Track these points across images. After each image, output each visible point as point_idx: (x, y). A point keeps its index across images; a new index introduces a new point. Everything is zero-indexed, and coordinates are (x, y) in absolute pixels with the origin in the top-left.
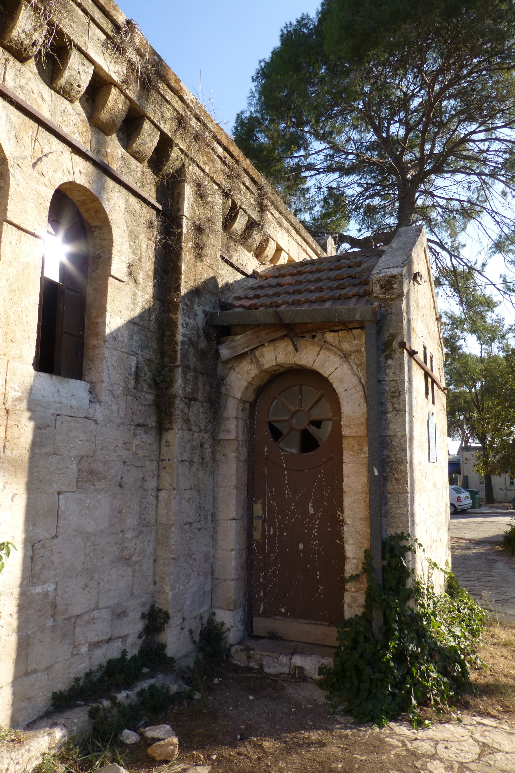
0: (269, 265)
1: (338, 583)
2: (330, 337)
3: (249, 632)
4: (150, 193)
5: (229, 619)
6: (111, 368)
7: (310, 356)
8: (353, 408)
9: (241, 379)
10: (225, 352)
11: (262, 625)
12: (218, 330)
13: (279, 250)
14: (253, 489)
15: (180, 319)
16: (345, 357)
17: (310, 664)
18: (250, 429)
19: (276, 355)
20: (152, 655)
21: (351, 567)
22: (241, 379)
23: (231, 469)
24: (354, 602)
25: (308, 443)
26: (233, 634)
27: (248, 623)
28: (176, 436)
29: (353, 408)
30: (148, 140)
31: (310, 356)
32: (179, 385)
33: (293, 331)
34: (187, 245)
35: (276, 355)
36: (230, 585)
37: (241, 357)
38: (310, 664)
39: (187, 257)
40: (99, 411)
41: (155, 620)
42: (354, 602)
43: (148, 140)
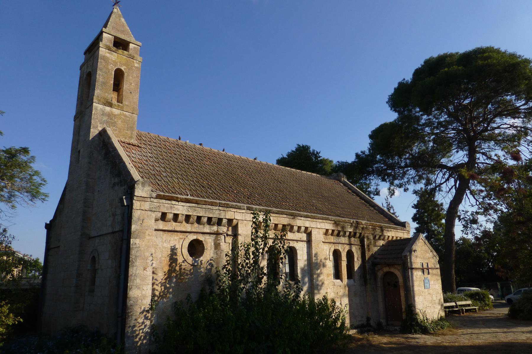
0: (386, 241)
2: (396, 266)
4: (359, 243)
5: (382, 321)
6: (356, 277)
7: (392, 270)
8: (401, 280)
9: (380, 274)
10: (376, 269)
12: (374, 265)
13: (389, 237)
15: (367, 265)
16: (399, 270)
17: (397, 328)
19: (386, 269)
20: (369, 325)
21: (403, 310)
22: (380, 274)
24: (404, 316)
29: (401, 280)
30: (358, 235)
33: (389, 265)
34: (366, 250)
35: (386, 269)
37: (379, 270)
38: (397, 328)
39: (367, 252)
40: (356, 284)
41: (368, 319)
42: (404, 316)
43: (358, 235)
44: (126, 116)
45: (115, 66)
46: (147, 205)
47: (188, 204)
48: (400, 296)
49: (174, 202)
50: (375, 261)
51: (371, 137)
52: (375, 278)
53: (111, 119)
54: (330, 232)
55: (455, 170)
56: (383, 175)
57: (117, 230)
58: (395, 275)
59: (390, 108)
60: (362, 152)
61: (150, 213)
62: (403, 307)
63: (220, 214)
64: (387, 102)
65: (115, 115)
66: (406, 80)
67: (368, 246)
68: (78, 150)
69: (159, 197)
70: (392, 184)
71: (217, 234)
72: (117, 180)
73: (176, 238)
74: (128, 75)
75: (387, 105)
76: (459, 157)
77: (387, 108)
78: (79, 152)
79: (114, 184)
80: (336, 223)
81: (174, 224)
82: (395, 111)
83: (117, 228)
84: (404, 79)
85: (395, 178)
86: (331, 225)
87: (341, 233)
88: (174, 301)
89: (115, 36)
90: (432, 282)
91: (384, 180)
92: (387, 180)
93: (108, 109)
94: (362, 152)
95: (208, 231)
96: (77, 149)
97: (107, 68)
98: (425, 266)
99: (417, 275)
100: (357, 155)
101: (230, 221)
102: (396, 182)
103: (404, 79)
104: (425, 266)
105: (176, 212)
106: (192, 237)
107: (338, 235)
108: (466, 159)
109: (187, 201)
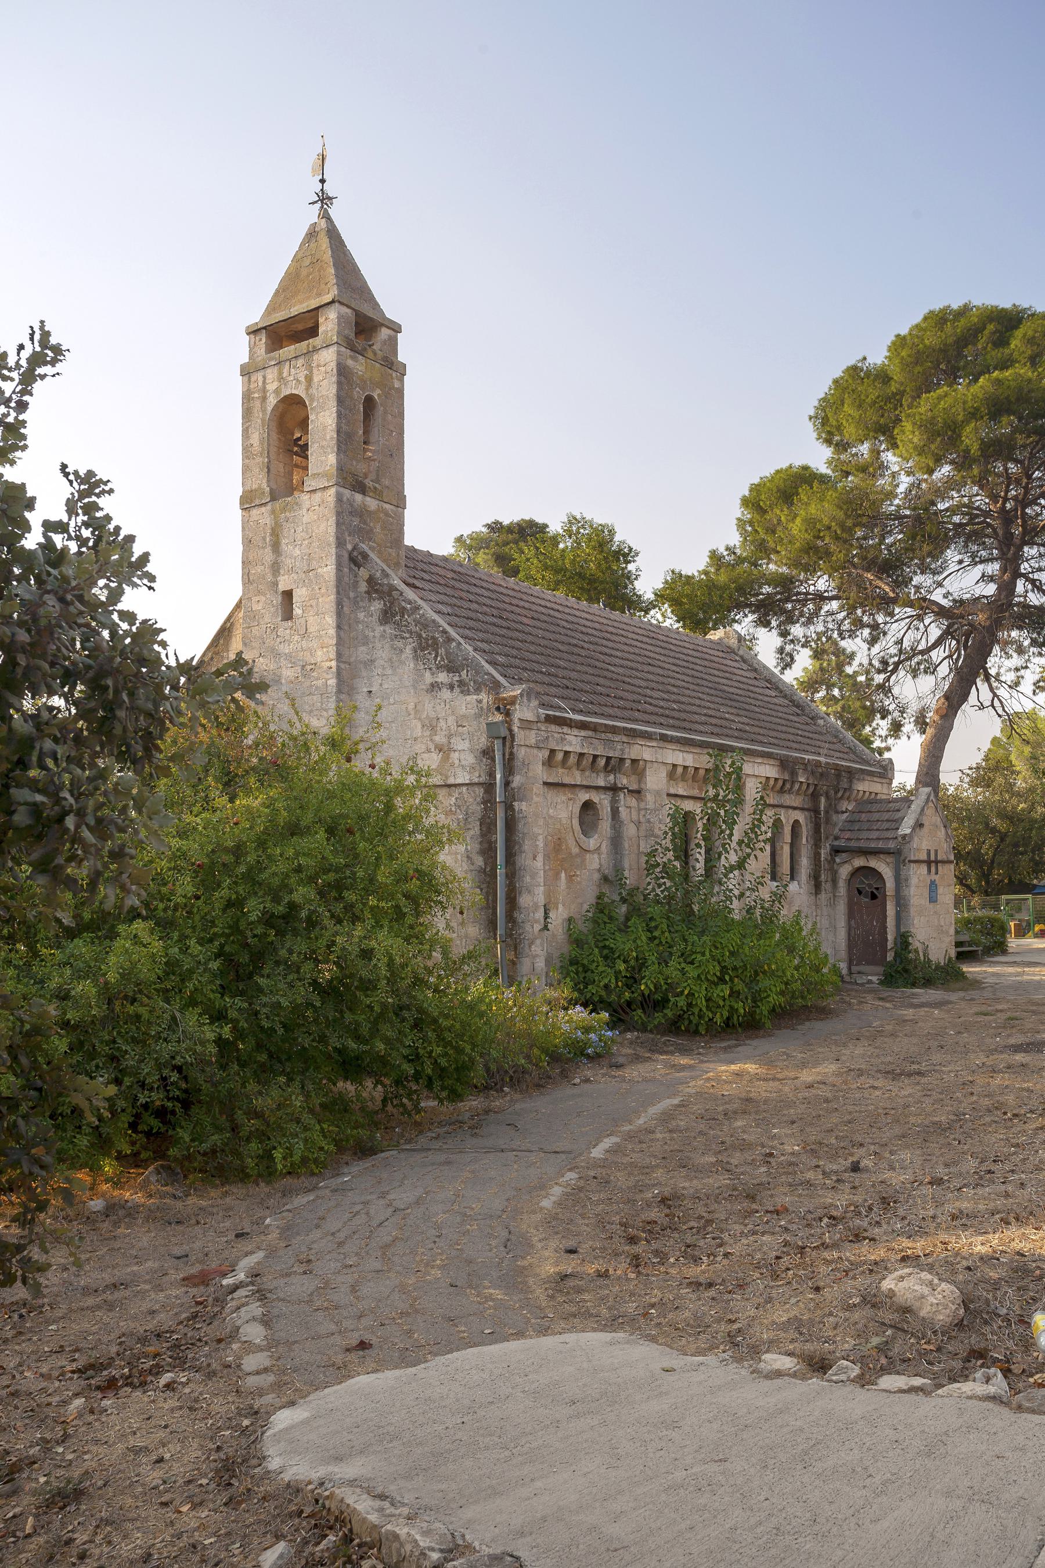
1: (885, 951)
3: (850, 973)
7: (873, 863)
9: (844, 871)
10: (838, 860)
11: (854, 969)
14: (851, 915)
17: (874, 979)
18: (849, 891)
19: (859, 862)
21: (890, 945)
23: (842, 908)
24: (890, 956)
25: (874, 897)
26: (844, 972)
27: (850, 969)
28: (823, 896)
29: (890, 885)
31: (873, 863)
32: (823, 877)
35: (859, 862)
36: (843, 954)
38: (874, 979)
42: (890, 956)
44: (387, 514)
45: (363, 389)
46: (532, 737)
47: (583, 733)
48: (885, 917)
49: (566, 729)
50: (836, 843)
51: (745, 502)
52: (834, 882)
53: (365, 523)
54: (772, 782)
55: (956, 617)
56: (766, 612)
57: (459, 781)
58: (879, 876)
59: (815, 435)
60: (728, 549)
61: (535, 751)
62: (890, 937)
63: (622, 750)
64: (810, 418)
65: (370, 513)
66: (870, 360)
67: (827, 812)
68: (282, 587)
69: (549, 719)
70: (784, 634)
71: (614, 789)
72: (443, 677)
73: (564, 798)
74: (385, 412)
75: (810, 425)
76: (964, 579)
77: (809, 431)
78: (288, 595)
79: (435, 687)
80: (784, 764)
81: (561, 770)
82: (828, 442)
83: (463, 778)
84: (865, 359)
85: (791, 620)
86: (776, 769)
87: (788, 786)
88: (565, 916)
89: (358, 314)
90: (940, 890)
91: (766, 624)
92: (774, 623)
93: (359, 497)
94: (728, 549)
95: (602, 783)
96: (276, 584)
97: (352, 398)
98: (933, 858)
99: (917, 875)
100: (714, 556)
101: (634, 761)
102: (797, 630)
103: (865, 359)
104: (933, 858)
105: (568, 748)
106: (584, 796)
107: (782, 791)
108: (991, 589)
109: (583, 726)
